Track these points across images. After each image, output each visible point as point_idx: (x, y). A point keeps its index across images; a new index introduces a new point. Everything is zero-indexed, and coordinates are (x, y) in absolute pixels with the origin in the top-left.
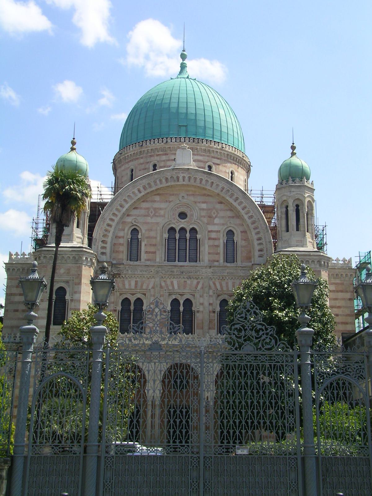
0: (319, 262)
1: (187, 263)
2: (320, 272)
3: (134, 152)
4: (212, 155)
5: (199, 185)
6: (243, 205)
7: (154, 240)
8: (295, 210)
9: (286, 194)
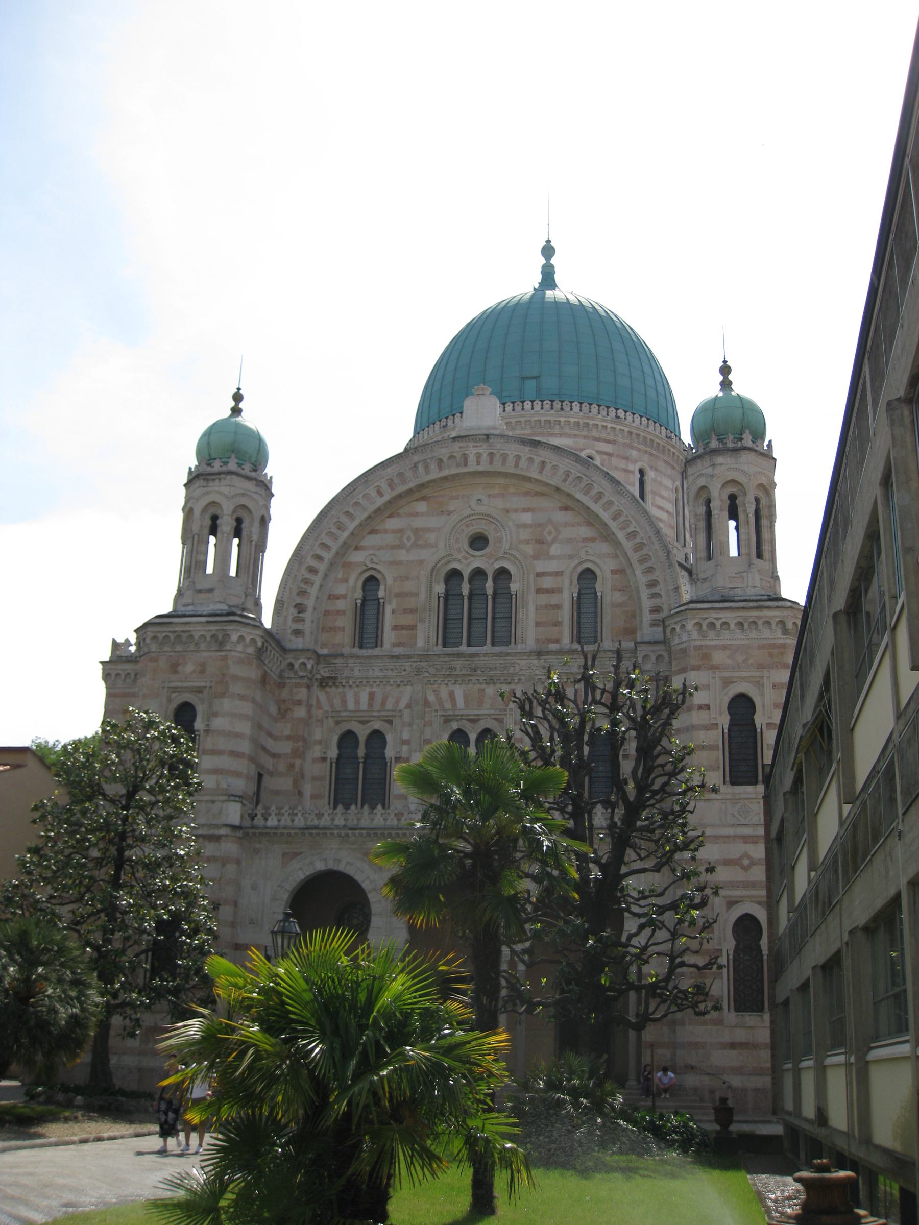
1: (488, 648)
4: (595, 433)
6: (614, 509)
9: (704, 471)
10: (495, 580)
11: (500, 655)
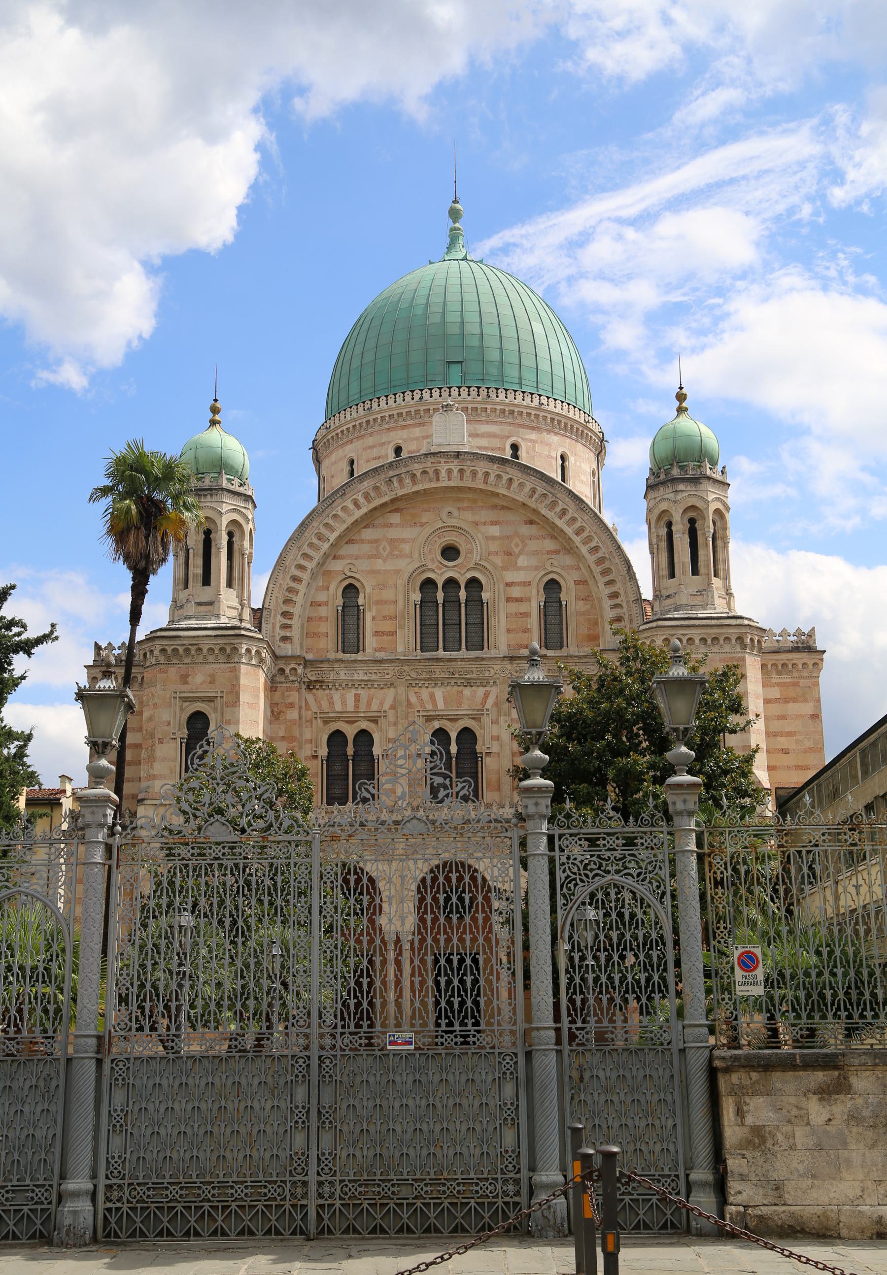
0: (740, 639)
1: (463, 653)
2: (743, 660)
3: (354, 424)
5: (482, 486)
6: (578, 525)
7: (392, 607)
8: (687, 532)
9: (666, 496)
10: (466, 588)
11: (477, 659)
